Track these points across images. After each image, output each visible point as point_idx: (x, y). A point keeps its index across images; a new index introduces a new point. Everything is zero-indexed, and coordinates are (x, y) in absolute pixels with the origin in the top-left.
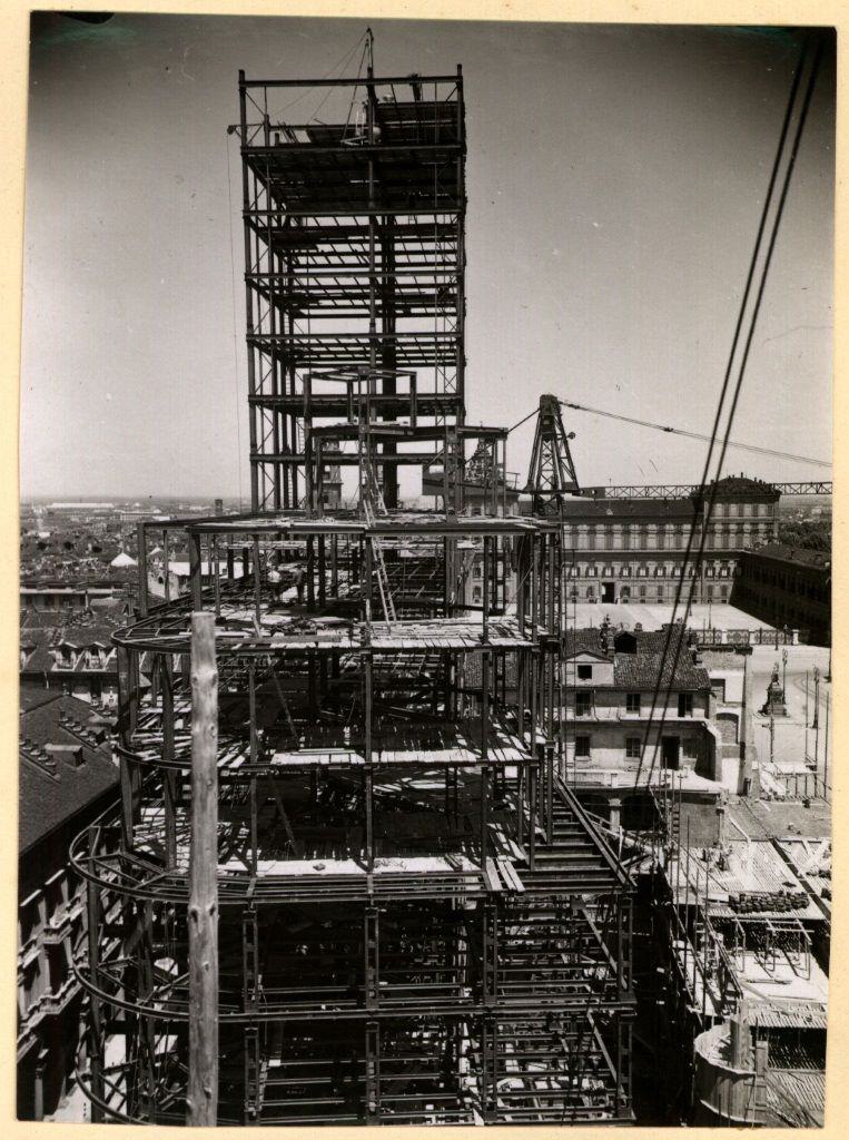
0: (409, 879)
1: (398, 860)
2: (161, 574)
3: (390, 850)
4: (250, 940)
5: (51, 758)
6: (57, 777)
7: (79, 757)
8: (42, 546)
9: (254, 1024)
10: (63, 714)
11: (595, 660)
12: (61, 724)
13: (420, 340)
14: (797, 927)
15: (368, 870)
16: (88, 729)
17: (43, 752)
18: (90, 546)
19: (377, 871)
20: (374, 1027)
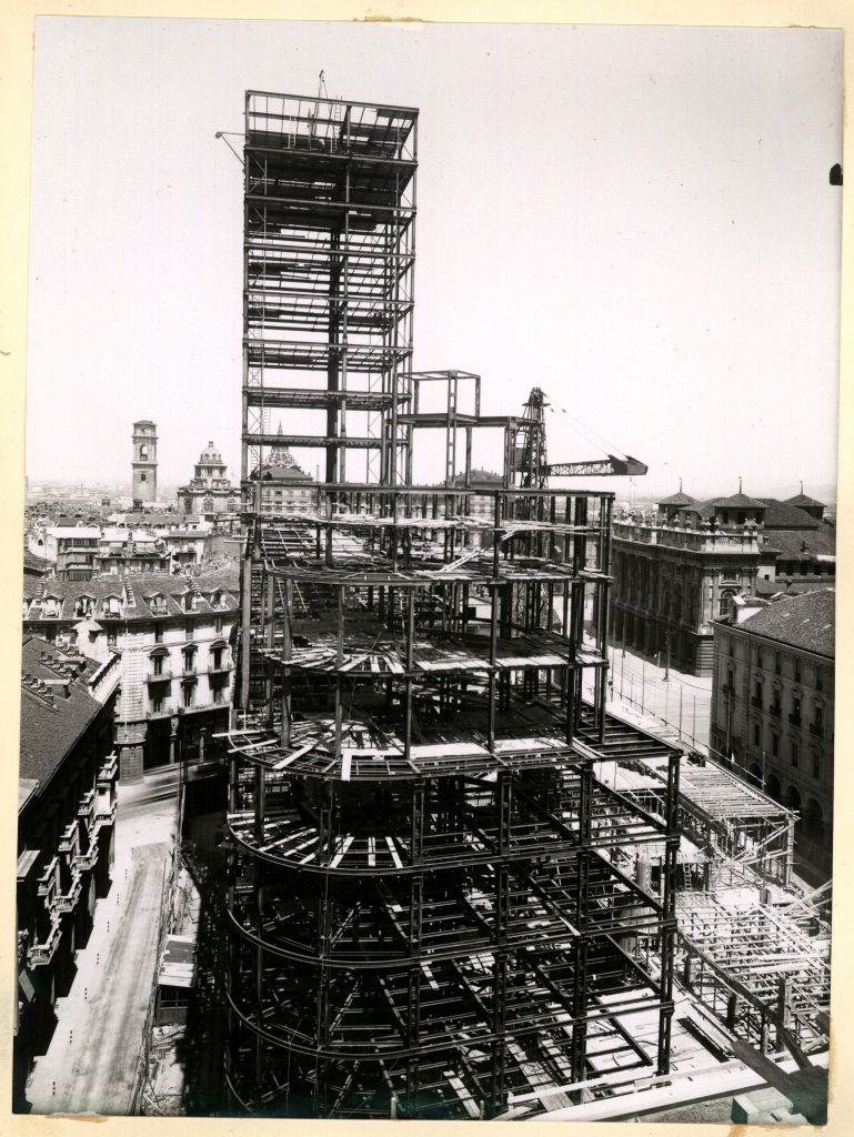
0: (521, 754)
1: (508, 742)
2: (41, 537)
3: (502, 735)
4: (418, 808)
5: (50, 690)
6: (55, 706)
7: (67, 692)
9: (419, 874)
10: (43, 654)
11: (478, 602)
12: (42, 662)
13: (283, 346)
14: (648, 794)
15: (490, 747)
16: (66, 666)
17: (43, 685)
19: (497, 750)
20: (419, 880)
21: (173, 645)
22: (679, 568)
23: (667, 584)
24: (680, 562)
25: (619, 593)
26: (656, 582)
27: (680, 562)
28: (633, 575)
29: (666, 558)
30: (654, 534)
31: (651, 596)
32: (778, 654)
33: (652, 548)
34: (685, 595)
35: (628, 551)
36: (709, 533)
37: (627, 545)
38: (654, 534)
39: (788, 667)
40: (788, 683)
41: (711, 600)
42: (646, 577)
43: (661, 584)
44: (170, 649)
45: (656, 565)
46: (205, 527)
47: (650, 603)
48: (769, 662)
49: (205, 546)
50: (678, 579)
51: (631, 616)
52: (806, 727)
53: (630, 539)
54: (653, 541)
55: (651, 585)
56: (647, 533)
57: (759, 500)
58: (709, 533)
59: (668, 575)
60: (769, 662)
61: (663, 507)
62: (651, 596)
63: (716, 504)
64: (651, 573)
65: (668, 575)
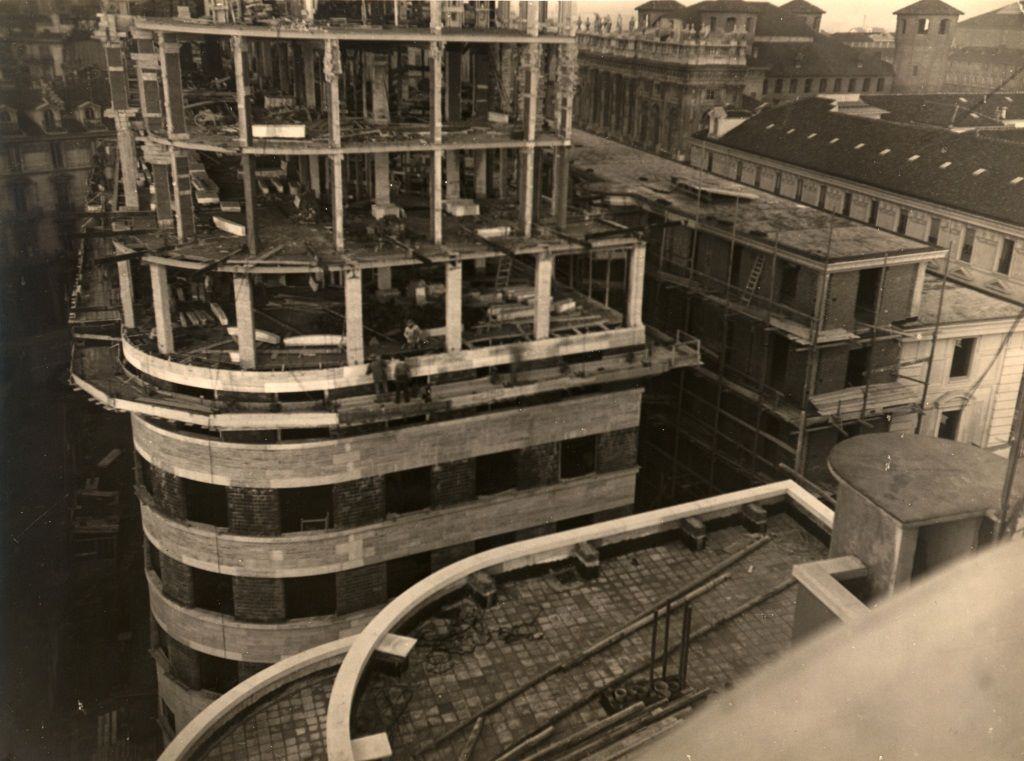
21: (37, 173)
22: (658, 86)
23: (645, 107)
25: (591, 119)
26: (632, 103)
28: (607, 97)
29: (644, 74)
31: (626, 121)
36: (693, 43)
41: (691, 122)
42: (620, 96)
43: (638, 106)
44: (34, 179)
46: (59, 27)
47: (625, 128)
49: (64, 52)
55: (627, 108)
58: (693, 43)
59: (645, 95)
64: (627, 94)
65: (645, 95)
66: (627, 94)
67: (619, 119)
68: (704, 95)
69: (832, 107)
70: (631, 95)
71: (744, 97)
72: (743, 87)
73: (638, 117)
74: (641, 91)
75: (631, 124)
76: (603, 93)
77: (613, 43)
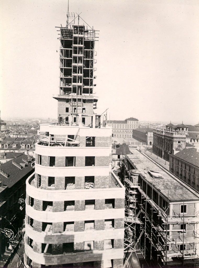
8: (19, 125)
18: (27, 126)
23: (167, 143)
24: (169, 139)
25: (157, 145)
26: (164, 143)
27: (169, 139)
28: (160, 141)
29: (166, 138)
30: (164, 132)
31: (163, 146)
32: (182, 162)
33: (164, 136)
34: (170, 146)
35: (159, 136)
37: (158, 134)
38: (164, 132)
39: (184, 165)
40: (184, 169)
42: (162, 142)
43: (165, 143)
45: (164, 139)
47: (163, 147)
48: (180, 164)
50: (169, 142)
51: (159, 150)
52: (187, 179)
53: (159, 133)
54: (164, 134)
56: (162, 132)
57: (187, 125)
59: (167, 141)
60: (180, 164)
61: (167, 126)
62: (163, 146)
63: (177, 126)
64: (163, 141)
65: (167, 141)
66: (163, 141)
67: (162, 145)
68: (178, 142)
69: (197, 150)
70: (164, 141)
71: (186, 143)
72: (186, 141)
73: (166, 146)
74: (165, 140)
75: (164, 146)
76: (159, 141)
77: (161, 132)
